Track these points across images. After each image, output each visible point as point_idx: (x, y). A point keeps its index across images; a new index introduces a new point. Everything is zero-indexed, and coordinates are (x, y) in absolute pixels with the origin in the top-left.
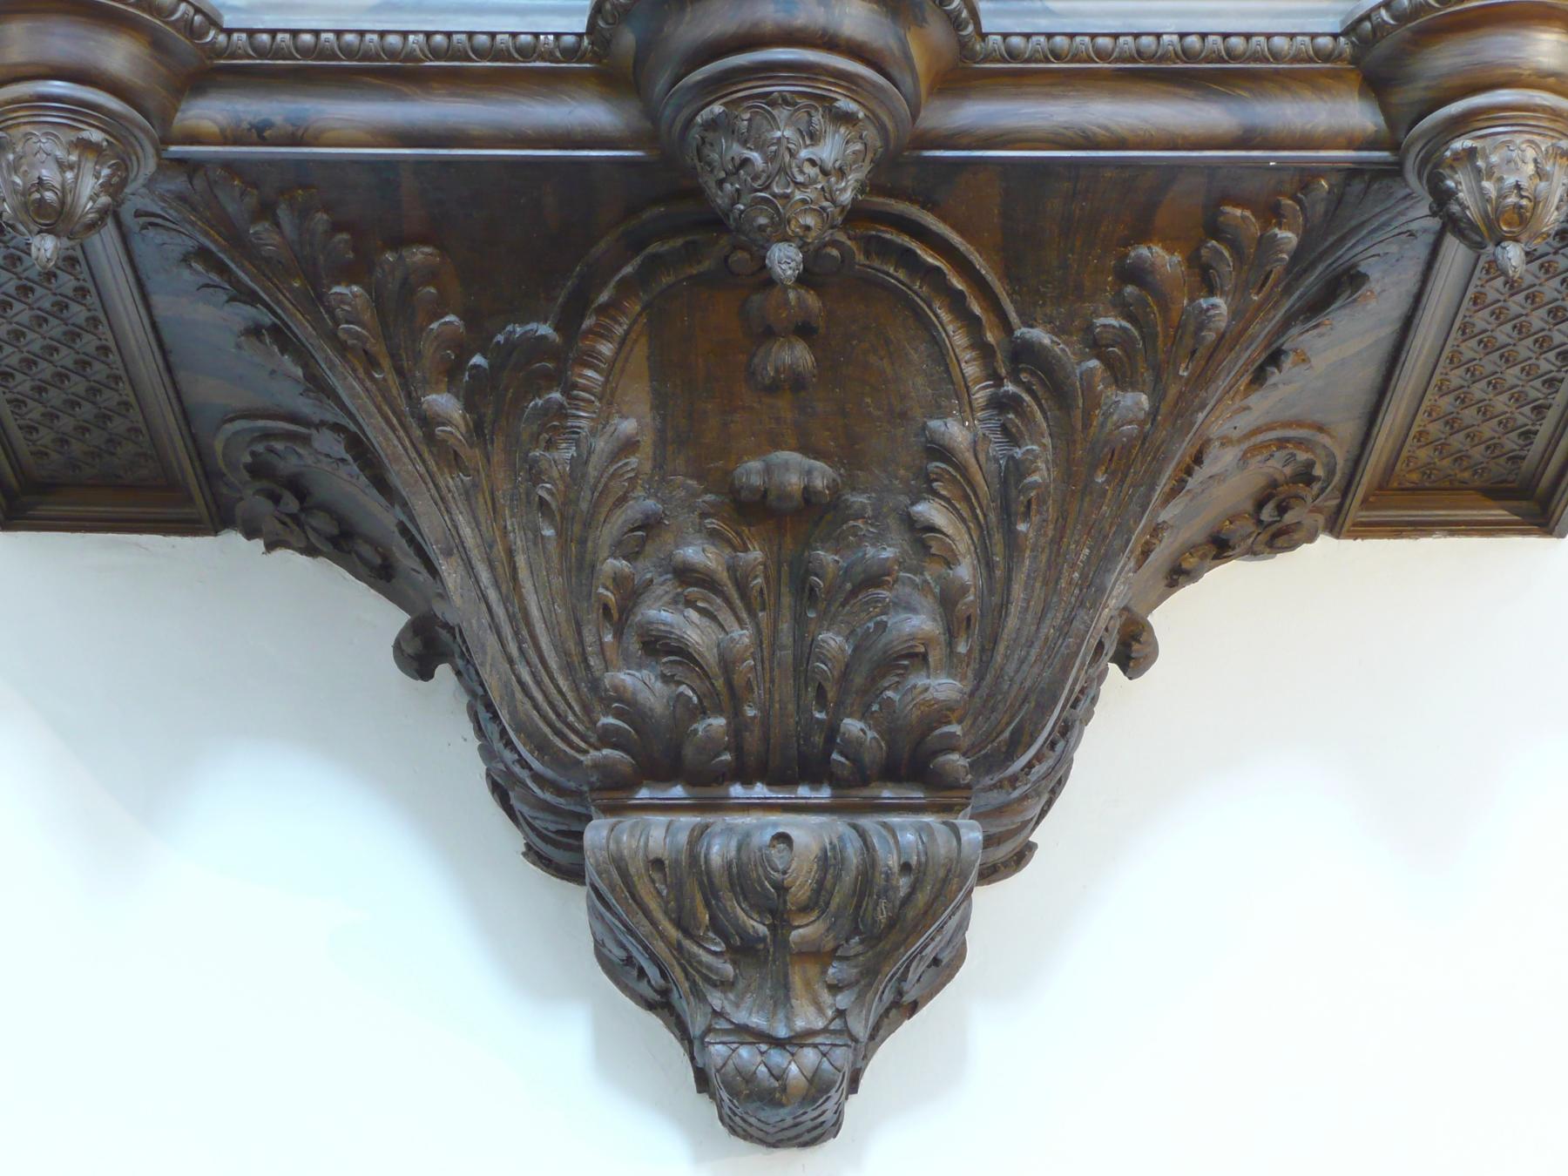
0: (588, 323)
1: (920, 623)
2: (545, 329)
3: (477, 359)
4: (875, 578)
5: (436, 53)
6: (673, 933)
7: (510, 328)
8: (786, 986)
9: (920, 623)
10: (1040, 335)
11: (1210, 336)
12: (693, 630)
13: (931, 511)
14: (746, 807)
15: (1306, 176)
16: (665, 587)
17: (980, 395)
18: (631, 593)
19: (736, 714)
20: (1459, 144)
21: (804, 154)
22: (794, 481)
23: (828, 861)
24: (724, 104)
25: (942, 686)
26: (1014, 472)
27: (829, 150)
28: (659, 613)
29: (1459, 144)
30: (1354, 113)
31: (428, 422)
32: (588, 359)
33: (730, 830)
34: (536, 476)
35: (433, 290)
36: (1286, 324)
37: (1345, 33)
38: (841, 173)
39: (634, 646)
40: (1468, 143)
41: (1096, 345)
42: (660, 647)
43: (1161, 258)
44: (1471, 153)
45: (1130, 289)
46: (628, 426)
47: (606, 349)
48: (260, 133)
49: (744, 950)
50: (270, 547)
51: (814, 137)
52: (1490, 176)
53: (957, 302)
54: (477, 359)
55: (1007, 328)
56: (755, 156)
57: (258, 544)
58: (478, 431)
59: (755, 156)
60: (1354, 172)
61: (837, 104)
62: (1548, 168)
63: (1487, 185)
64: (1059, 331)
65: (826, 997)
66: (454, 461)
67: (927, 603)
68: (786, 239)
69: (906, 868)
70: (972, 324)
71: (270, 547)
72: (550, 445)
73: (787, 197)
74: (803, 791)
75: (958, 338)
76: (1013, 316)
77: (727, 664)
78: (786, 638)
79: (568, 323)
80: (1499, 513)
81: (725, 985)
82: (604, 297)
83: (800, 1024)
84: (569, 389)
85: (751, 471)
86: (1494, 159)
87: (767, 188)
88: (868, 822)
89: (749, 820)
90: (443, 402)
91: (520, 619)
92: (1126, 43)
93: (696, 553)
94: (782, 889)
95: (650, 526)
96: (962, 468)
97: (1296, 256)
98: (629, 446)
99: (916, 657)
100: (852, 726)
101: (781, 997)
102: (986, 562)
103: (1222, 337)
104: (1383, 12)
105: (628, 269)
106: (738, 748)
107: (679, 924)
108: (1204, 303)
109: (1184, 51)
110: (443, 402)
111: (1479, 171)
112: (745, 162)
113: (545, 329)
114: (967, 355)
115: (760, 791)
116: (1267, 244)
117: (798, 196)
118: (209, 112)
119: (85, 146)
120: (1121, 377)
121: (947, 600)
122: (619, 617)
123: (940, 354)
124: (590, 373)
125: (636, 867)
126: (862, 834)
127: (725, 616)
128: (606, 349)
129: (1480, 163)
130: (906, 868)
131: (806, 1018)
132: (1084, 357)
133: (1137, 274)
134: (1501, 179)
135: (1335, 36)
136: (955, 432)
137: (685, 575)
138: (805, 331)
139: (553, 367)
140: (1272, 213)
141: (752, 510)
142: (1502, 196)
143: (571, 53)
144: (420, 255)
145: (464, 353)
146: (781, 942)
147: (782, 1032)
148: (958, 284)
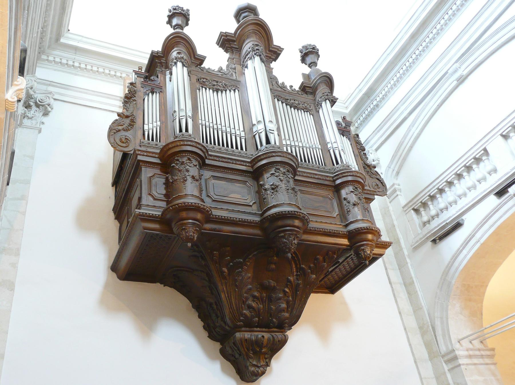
0: (247, 260)
1: (284, 305)
2: (241, 260)
4: (280, 299)
5: (239, 221)
6: (246, 350)
8: (260, 358)
9: (284, 305)
10: (303, 266)
12: (254, 304)
13: (287, 290)
14: (256, 331)
15: (339, 249)
16: (251, 299)
17: (295, 274)
18: (247, 299)
19: (259, 318)
20: (362, 248)
22: (272, 284)
23: (269, 339)
25: (287, 315)
26: (298, 285)
28: (250, 302)
29: (362, 248)
30: (345, 241)
31: (223, 272)
32: (246, 265)
33: (255, 335)
34: (236, 280)
39: (246, 307)
41: (310, 268)
42: (250, 307)
46: (250, 275)
47: (248, 264)
48: (214, 230)
49: (255, 353)
50: (164, 286)
54: (231, 264)
57: (162, 285)
58: (229, 274)
65: (264, 360)
66: (225, 278)
67: (285, 302)
69: (279, 341)
71: (164, 286)
72: (238, 277)
74: (264, 329)
77: (259, 310)
78: (267, 307)
79: (244, 260)
80: (327, 291)
81: (252, 358)
83: (261, 364)
84: (242, 268)
85: (266, 282)
88: (273, 334)
89: (256, 333)
90: (225, 269)
91: (231, 303)
92: (314, 229)
93: (256, 294)
94: (262, 344)
95: (250, 289)
96: (292, 284)
98: (249, 278)
99: (283, 310)
100: (274, 320)
101: (259, 361)
102: (293, 298)
106: (258, 323)
107: (247, 349)
110: (225, 269)
113: (241, 260)
115: (258, 329)
118: (208, 226)
119: (196, 230)
120: (312, 273)
121: (288, 302)
122: (244, 303)
123: (292, 268)
125: (243, 341)
126: (273, 336)
127: (259, 303)
128: (248, 264)
130: (279, 341)
131: (262, 363)
133: (317, 259)
136: (291, 278)
137: (254, 297)
138: (275, 264)
139: (240, 265)
140: (334, 253)
141: (264, 288)
143: (256, 223)
144: (228, 248)
146: (260, 351)
147: (260, 365)
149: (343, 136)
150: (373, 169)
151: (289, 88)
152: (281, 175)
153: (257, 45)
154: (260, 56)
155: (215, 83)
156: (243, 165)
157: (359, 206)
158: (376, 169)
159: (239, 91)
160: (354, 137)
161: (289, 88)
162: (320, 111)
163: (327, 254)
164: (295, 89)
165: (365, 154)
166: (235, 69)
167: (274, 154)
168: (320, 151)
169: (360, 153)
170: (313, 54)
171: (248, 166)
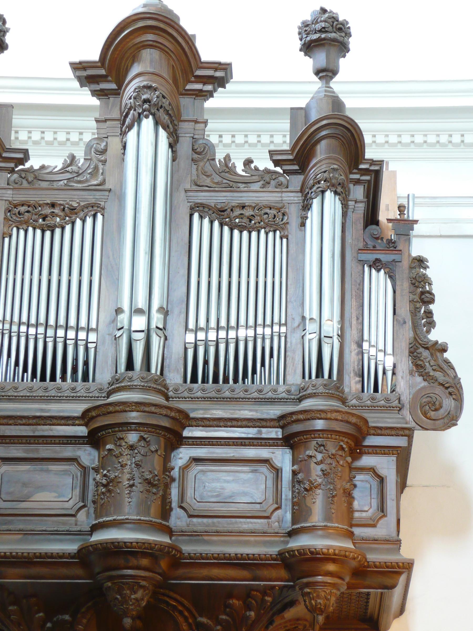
0: (79, 616)
2: (67, 617)
3: (49, 625)
7: (58, 617)
11: (250, 622)
15: (273, 587)
21: (133, 597)
24: (111, 583)
27: (139, 594)
35: (36, 608)
36: (274, 615)
37: (279, 555)
38: (142, 599)
40: (308, 590)
41: (219, 622)
43: (235, 602)
44: (309, 593)
45: (228, 610)
51: (135, 593)
52: (313, 599)
53: (181, 613)
54: (49, 625)
55: (195, 618)
56: (118, 597)
59: (118, 597)
60: (285, 586)
61: (141, 584)
62: (329, 597)
63: (313, 602)
64: (209, 619)
68: (127, 617)
70: (186, 619)
73: (127, 608)
75: (180, 619)
76: (197, 615)
82: (83, 610)
86: (315, 595)
87: (122, 606)
97: (271, 603)
103: (254, 621)
104: (287, 554)
105: (90, 604)
108: (248, 613)
109: (236, 558)
111: (311, 598)
112: (117, 598)
113: (67, 617)
114: (184, 624)
116: (263, 600)
117: (131, 607)
124: (80, 627)
128: (85, 621)
129: (311, 596)
132: (216, 625)
134: (316, 601)
135: (277, 555)
142: (316, 605)
143: (73, 557)
145: (45, 624)
148: (180, 608)
149: (378, 271)
150: (438, 354)
151: (240, 169)
152: (127, 451)
153: (149, 87)
154: (154, 115)
155: (48, 211)
156: (68, 425)
157: (319, 491)
158: (446, 355)
159: (103, 215)
160: (411, 268)
161: (240, 169)
162: (308, 222)
163: (249, 596)
164: (256, 169)
165: (429, 314)
166: (104, 152)
167: (111, 409)
168: (283, 339)
169: (414, 312)
170: (323, 45)
171: (79, 425)
